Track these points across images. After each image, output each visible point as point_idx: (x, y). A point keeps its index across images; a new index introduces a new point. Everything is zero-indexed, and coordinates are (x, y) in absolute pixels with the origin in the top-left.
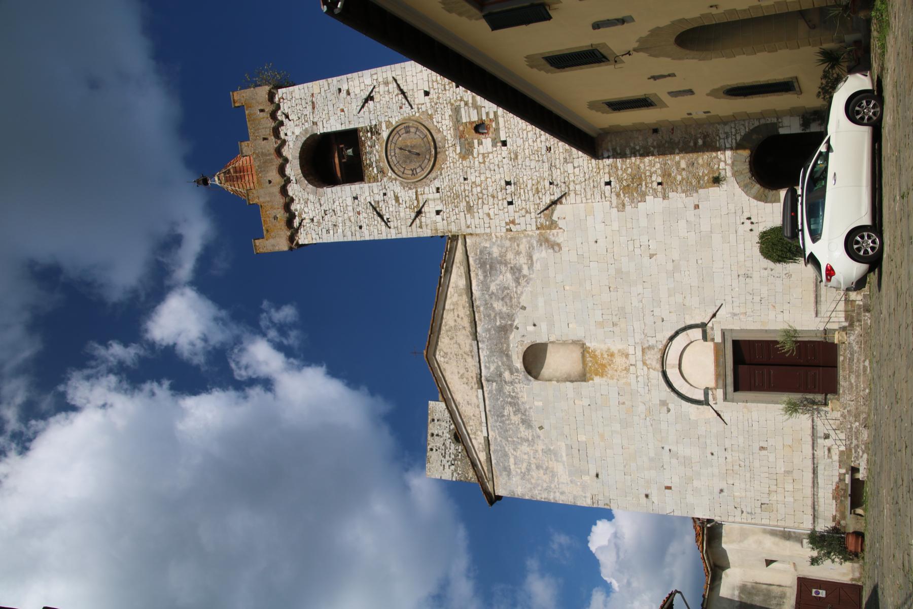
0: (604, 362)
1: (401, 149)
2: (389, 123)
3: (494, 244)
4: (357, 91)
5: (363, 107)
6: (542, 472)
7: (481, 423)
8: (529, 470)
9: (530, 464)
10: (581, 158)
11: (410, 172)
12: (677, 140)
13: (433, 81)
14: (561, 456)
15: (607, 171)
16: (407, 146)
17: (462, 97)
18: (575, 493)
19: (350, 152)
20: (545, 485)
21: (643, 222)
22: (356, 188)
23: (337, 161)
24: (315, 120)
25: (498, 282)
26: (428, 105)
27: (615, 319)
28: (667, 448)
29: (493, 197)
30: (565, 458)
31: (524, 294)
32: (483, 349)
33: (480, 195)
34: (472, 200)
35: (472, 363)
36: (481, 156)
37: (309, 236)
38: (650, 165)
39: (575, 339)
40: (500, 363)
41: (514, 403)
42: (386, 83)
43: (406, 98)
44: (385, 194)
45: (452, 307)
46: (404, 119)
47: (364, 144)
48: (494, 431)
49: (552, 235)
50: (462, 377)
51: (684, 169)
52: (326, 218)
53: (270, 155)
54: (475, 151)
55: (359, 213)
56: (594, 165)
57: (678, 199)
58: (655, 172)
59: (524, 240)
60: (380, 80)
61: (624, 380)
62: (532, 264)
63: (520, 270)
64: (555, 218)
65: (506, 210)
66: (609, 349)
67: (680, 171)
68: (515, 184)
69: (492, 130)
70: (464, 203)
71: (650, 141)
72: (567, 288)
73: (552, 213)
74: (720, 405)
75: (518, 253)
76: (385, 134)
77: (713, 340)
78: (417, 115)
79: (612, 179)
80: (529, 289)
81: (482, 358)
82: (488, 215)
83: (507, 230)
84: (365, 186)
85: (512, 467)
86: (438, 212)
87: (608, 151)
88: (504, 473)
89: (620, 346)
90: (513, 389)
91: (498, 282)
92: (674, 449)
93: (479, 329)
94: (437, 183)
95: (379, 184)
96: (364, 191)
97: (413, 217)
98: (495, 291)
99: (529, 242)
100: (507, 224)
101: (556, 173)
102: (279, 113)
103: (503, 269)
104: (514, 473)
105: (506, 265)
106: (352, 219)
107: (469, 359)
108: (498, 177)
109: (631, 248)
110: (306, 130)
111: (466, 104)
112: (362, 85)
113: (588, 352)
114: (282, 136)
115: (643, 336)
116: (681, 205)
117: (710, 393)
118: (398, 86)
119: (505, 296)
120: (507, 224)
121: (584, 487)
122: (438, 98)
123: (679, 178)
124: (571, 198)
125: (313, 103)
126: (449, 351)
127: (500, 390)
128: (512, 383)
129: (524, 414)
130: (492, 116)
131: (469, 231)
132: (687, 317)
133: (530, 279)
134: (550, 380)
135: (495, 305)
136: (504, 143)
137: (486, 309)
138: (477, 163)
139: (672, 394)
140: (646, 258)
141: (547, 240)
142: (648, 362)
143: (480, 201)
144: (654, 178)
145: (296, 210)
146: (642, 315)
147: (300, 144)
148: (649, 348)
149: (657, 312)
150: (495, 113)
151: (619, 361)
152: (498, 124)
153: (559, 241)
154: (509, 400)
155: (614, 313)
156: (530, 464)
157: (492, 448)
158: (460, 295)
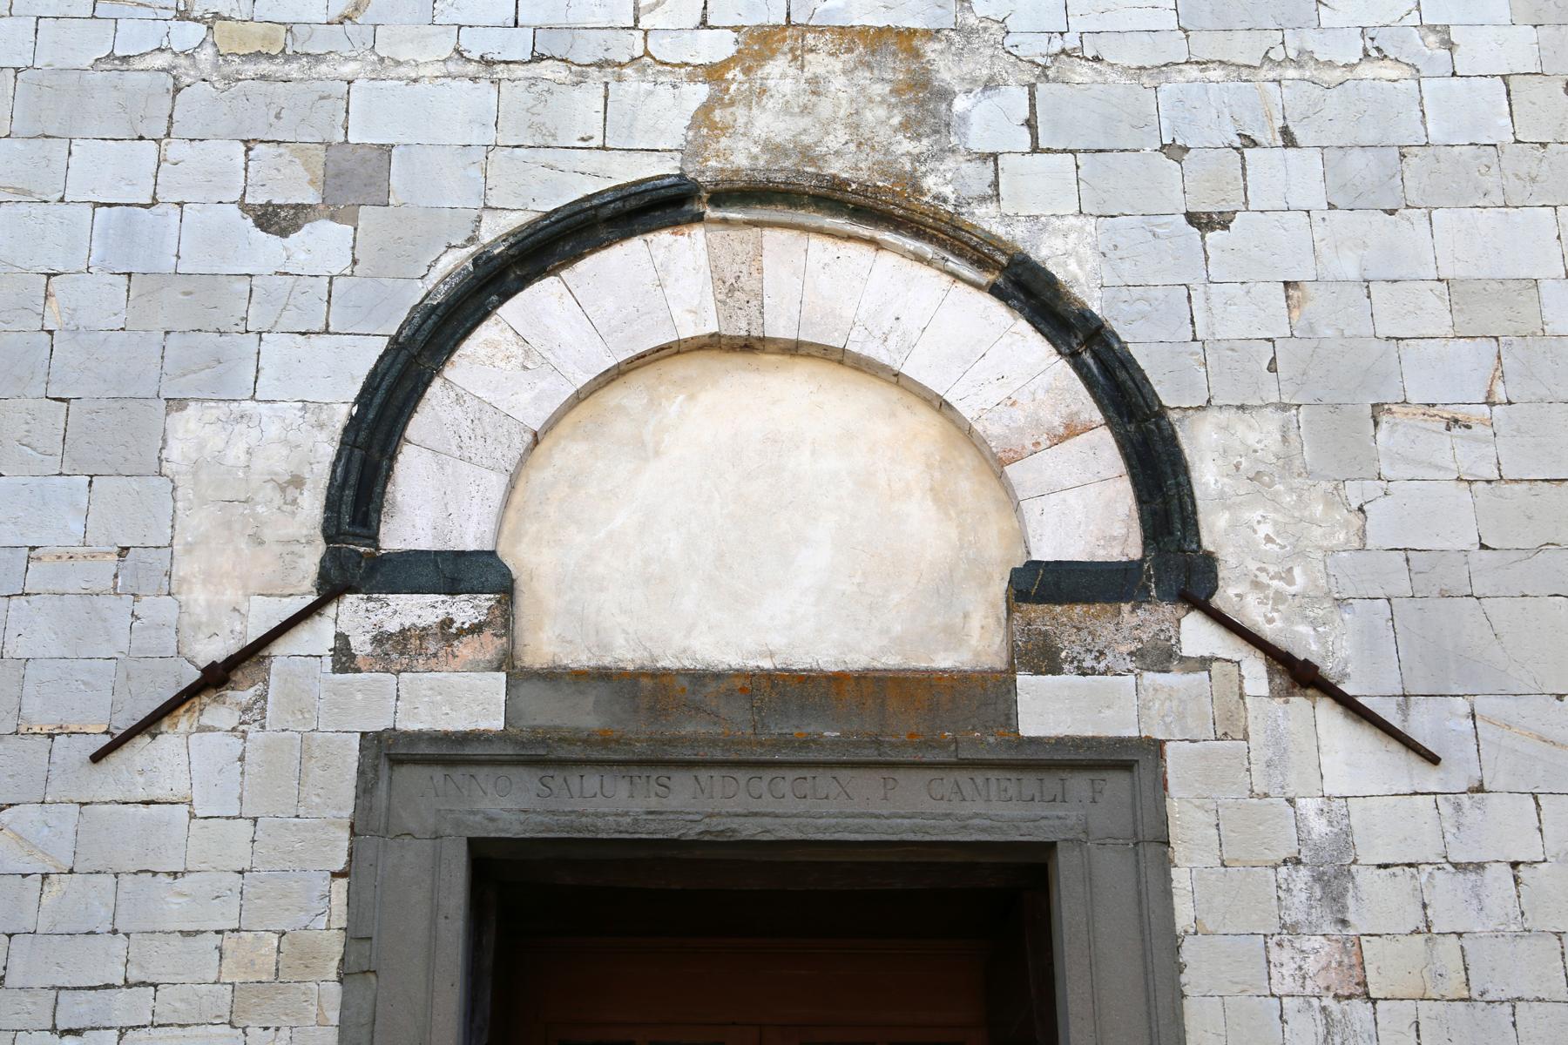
74: (325, 705)
77: (1045, 659)
115: (1035, 48)
117: (466, 609)
132: (1262, 434)
139: (454, 260)
142: (777, 72)
146: (1244, 49)
148: (924, 101)
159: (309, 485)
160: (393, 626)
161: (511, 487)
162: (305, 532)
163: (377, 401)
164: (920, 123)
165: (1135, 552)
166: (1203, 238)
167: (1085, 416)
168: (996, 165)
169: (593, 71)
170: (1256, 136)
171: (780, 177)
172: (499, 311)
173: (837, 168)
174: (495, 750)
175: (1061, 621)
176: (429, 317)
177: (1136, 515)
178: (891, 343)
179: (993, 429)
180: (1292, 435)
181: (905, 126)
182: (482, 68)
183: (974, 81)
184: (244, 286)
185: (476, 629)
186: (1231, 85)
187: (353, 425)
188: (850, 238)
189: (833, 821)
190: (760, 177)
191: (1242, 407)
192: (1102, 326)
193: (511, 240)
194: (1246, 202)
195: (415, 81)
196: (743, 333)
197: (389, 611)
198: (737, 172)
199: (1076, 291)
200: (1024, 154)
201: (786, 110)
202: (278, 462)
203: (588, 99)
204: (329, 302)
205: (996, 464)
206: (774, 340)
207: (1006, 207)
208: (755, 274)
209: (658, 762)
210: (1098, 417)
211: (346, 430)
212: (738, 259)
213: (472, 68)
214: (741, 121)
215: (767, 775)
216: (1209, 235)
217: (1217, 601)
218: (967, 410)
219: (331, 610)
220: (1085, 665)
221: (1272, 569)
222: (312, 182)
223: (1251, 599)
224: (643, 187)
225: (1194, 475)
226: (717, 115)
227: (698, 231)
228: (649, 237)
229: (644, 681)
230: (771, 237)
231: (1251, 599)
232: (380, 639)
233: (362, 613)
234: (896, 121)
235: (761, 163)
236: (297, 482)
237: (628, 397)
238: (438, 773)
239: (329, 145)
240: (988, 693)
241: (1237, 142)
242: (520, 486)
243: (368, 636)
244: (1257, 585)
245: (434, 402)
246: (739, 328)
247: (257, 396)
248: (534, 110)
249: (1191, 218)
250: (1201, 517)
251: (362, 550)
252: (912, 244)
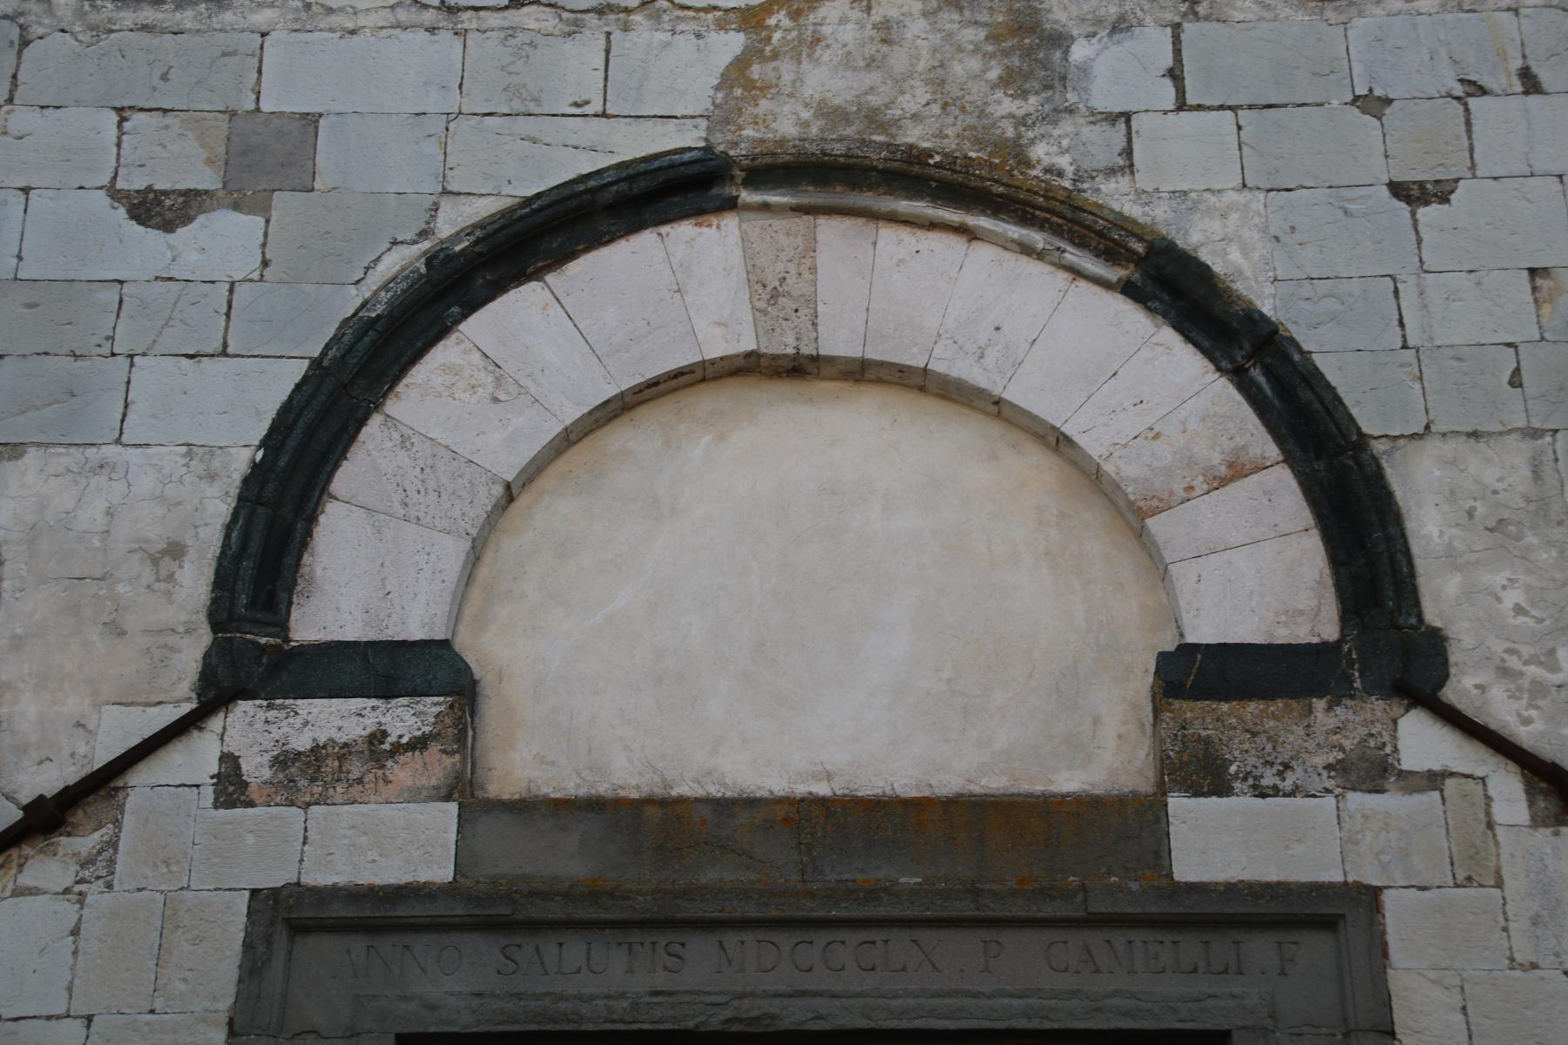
77: (1205, 773)
117: (404, 718)
132: (1503, 470)
159: (192, 554)
160: (302, 743)
161: (475, 557)
162: (183, 617)
163: (292, 443)
164: (1027, 76)
165: (1330, 631)
166: (1413, 214)
167: (1255, 452)
168: (1129, 127)
169: (591, 19)
170: (1486, 81)
171: (839, 149)
172: (463, 327)
173: (914, 135)
174: (440, 909)
175: (1228, 722)
176: (365, 333)
177: (1329, 581)
178: (991, 356)
179: (1128, 469)
180: (1547, 470)
181: (1005, 81)
182: (442, 16)
183: (1099, 22)
184: (110, 296)
185: (419, 744)
186: (1448, 17)
187: (256, 477)
188: (933, 225)
189: (912, 1002)
190: (813, 148)
191: (1474, 435)
192: (1276, 332)
193: (478, 233)
194: (1473, 167)
195: (353, 32)
196: (790, 351)
197: (298, 721)
198: (782, 142)
199: (1239, 287)
200: (1166, 112)
201: (847, 63)
202: (152, 526)
203: (584, 54)
204: (228, 315)
205: (1133, 516)
206: (831, 360)
207: (1143, 180)
208: (807, 275)
209: (667, 922)
210: (1273, 451)
211: (246, 481)
212: (783, 256)
213: (429, 17)
214: (787, 78)
215: (821, 938)
216: (1422, 212)
217: (1449, 694)
218: (1093, 445)
219: (216, 723)
220: (1264, 782)
221: (1526, 651)
222: (209, 162)
223: (1498, 693)
224: (656, 164)
225: (1410, 525)
226: (756, 71)
227: (730, 223)
228: (664, 229)
229: (650, 811)
230: (830, 231)
231: (1498, 693)
232: (283, 760)
233: (259, 725)
234: (994, 74)
235: (814, 131)
236: (175, 551)
237: (635, 438)
238: (358, 945)
239: (233, 114)
241: (1459, 90)
242: (488, 558)
243: (267, 757)
244: (1504, 672)
245: (370, 445)
246: (784, 344)
247: (125, 439)
248: (511, 68)
249: (1398, 190)
250: (1422, 582)
251: (263, 640)
252: (1015, 231)
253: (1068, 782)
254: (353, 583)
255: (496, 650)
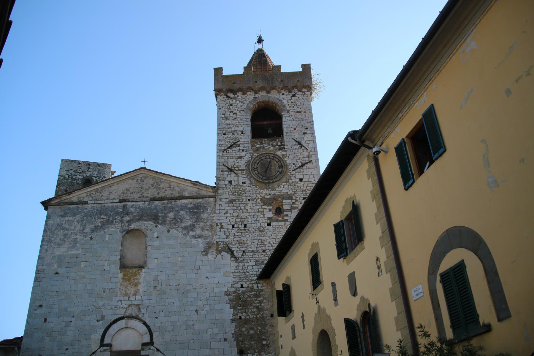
0: (132, 280)
1: (270, 162)
2: (285, 156)
3: (209, 215)
4: (306, 139)
5: (296, 141)
6: (62, 237)
7: (97, 200)
8: (64, 229)
9: (68, 230)
10: (258, 270)
11: (255, 167)
12: (266, 328)
13: (308, 184)
14: (71, 251)
15: (250, 286)
16: (271, 166)
17: (298, 201)
18: (46, 258)
19: (270, 131)
20: (53, 239)
21: (217, 307)
22: (249, 133)
23: (265, 123)
24: (290, 112)
25: (186, 216)
26: (294, 180)
27: (159, 288)
28: (73, 319)
29: (238, 216)
30: (70, 253)
31: (177, 232)
32: (144, 204)
33: (239, 208)
34: (237, 203)
35: (136, 196)
36: (262, 210)
37: (222, 102)
38: (252, 312)
39: (148, 263)
40: (134, 214)
41: (109, 222)
42: (308, 156)
43: (299, 167)
44: (243, 151)
45: (172, 187)
46: (287, 166)
47: (275, 140)
48: (91, 208)
49: (213, 251)
50: (127, 190)
51: (249, 332)
52: (232, 114)
53: (272, 83)
54: (266, 207)
55: (233, 134)
56: (253, 278)
57: (231, 328)
58: (248, 315)
59: (210, 234)
60: (311, 153)
61: (119, 293)
62: (196, 238)
63: (192, 230)
64: (223, 253)
65: (229, 223)
66: (140, 283)
67: (248, 330)
68: (245, 229)
69: (277, 217)
70: (234, 199)
71: (266, 312)
72: (180, 259)
73: (226, 252)
75: (203, 229)
76: (279, 153)
77: (143, 349)
78: (289, 174)
79: (244, 289)
80: (180, 235)
81: (139, 203)
82: (227, 213)
83: (217, 224)
84: (249, 139)
85: (67, 218)
86: (230, 182)
87: (262, 287)
88: (62, 213)
89: (141, 291)
90: (117, 222)
91: (186, 216)
92: (72, 324)
93: (157, 202)
94: (248, 182)
95: (250, 148)
96: (246, 138)
97: (229, 166)
98: (180, 214)
99: (209, 236)
100: (221, 224)
101: (249, 255)
102: (296, 91)
103: (194, 220)
104: (62, 219)
105: (195, 222)
106: (230, 130)
107: (138, 195)
108: (250, 220)
109: (202, 299)
110: (285, 106)
111: (294, 203)
112: (308, 142)
113: (138, 271)
114: (283, 92)
115: (147, 305)
116: (227, 330)
117: (108, 348)
118: (307, 163)
119: (178, 220)
120: (221, 224)
121: (49, 265)
122: (298, 187)
123: (244, 329)
124: (234, 264)
125: (300, 112)
126: (145, 183)
127: (117, 214)
128: (122, 221)
129: (101, 228)
130: (286, 218)
131: (218, 200)
132: (158, 333)
133: (186, 236)
134: (122, 246)
135: (171, 213)
136: (269, 225)
137: (169, 208)
138: (258, 207)
139: (109, 323)
140: (195, 308)
141: (209, 248)
142: (130, 308)
143: (236, 208)
144: (244, 314)
145: (238, 96)
147: (277, 101)
148: (139, 309)
149: (162, 314)
150: (287, 220)
151: (132, 290)
152: (281, 221)
153: (208, 255)
154: (111, 219)
155: (162, 288)
156: (68, 230)
157: (80, 206)
158: (179, 192)
237: (120, 331)
240: (140, 351)
253: (138, 349)
254: (107, 341)
255: (113, 343)
